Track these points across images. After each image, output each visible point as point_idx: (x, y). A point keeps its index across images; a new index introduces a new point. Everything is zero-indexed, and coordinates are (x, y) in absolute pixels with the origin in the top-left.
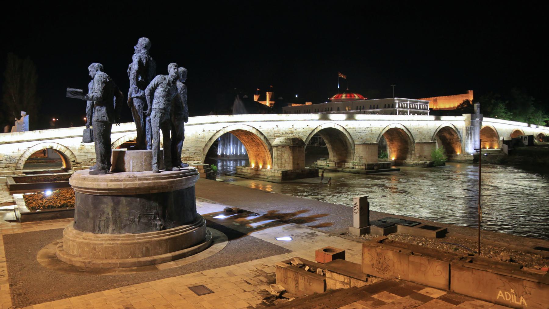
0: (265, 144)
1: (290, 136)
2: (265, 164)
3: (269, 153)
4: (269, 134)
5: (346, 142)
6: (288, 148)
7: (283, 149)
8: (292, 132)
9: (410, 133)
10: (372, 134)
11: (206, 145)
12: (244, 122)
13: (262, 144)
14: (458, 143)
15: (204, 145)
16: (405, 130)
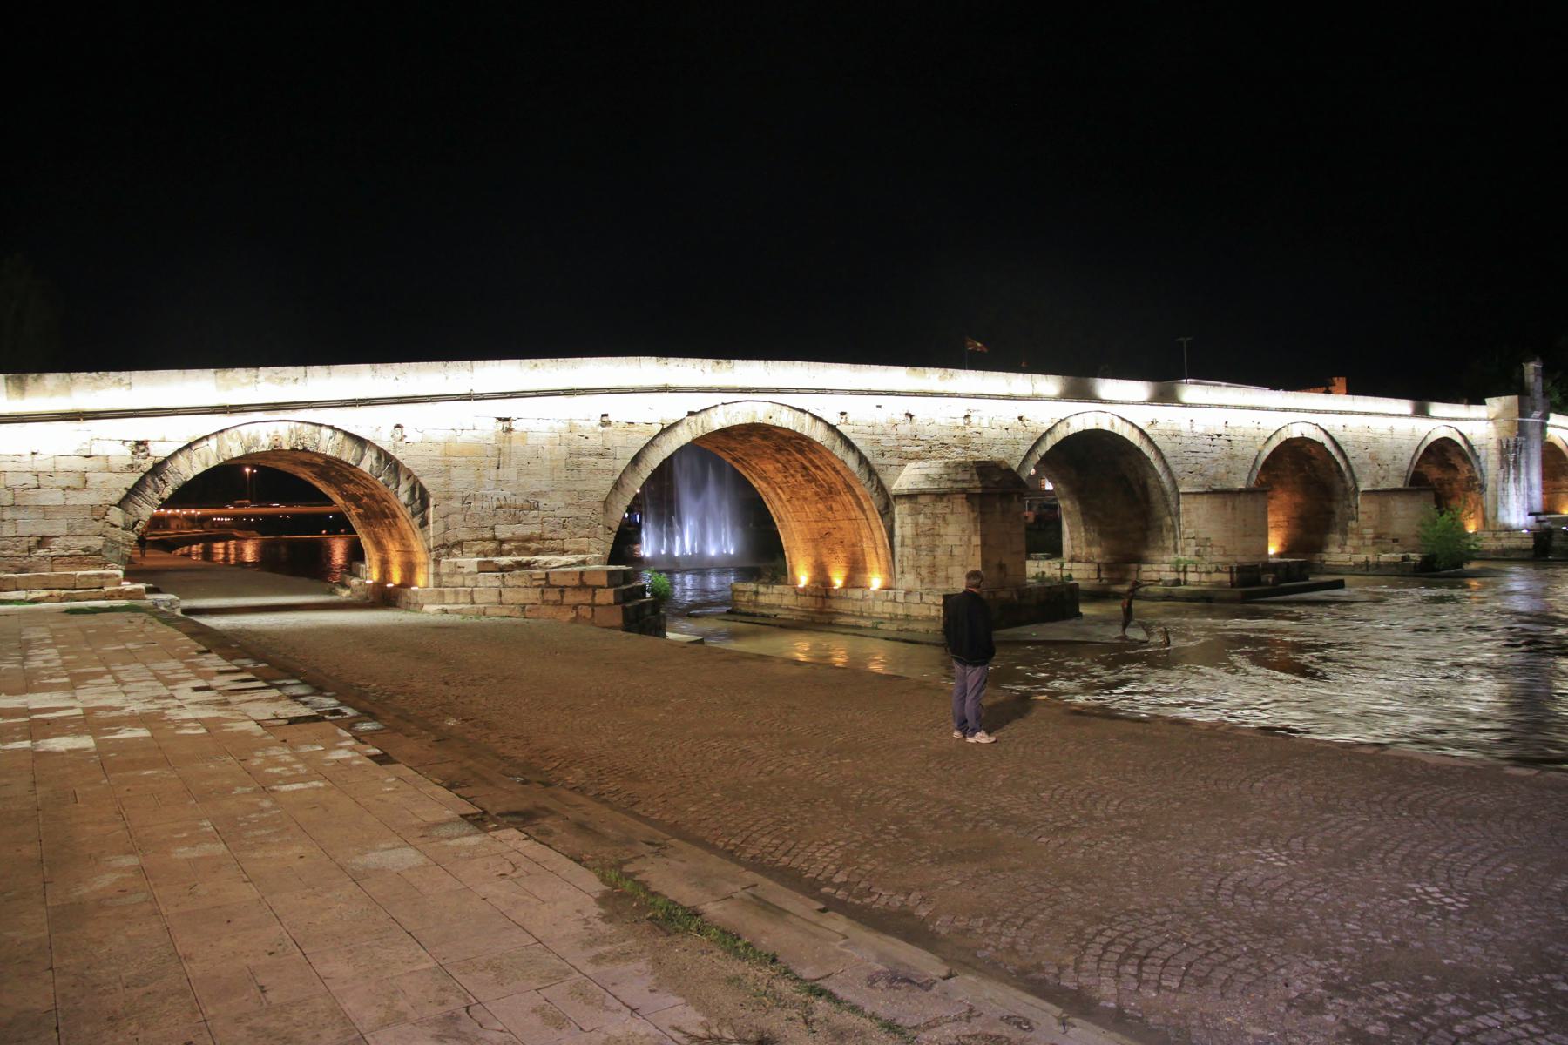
0: (864, 489)
1: (957, 455)
2: (856, 569)
3: (877, 524)
4: (877, 448)
5: (1144, 487)
6: (959, 501)
7: (940, 508)
8: (965, 443)
9: (1344, 456)
10: (1232, 457)
11: (617, 486)
12: (778, 391)
13: (850, 488)
14: (1473, 496)
15: (606, 483)
16: (1329, 445)
